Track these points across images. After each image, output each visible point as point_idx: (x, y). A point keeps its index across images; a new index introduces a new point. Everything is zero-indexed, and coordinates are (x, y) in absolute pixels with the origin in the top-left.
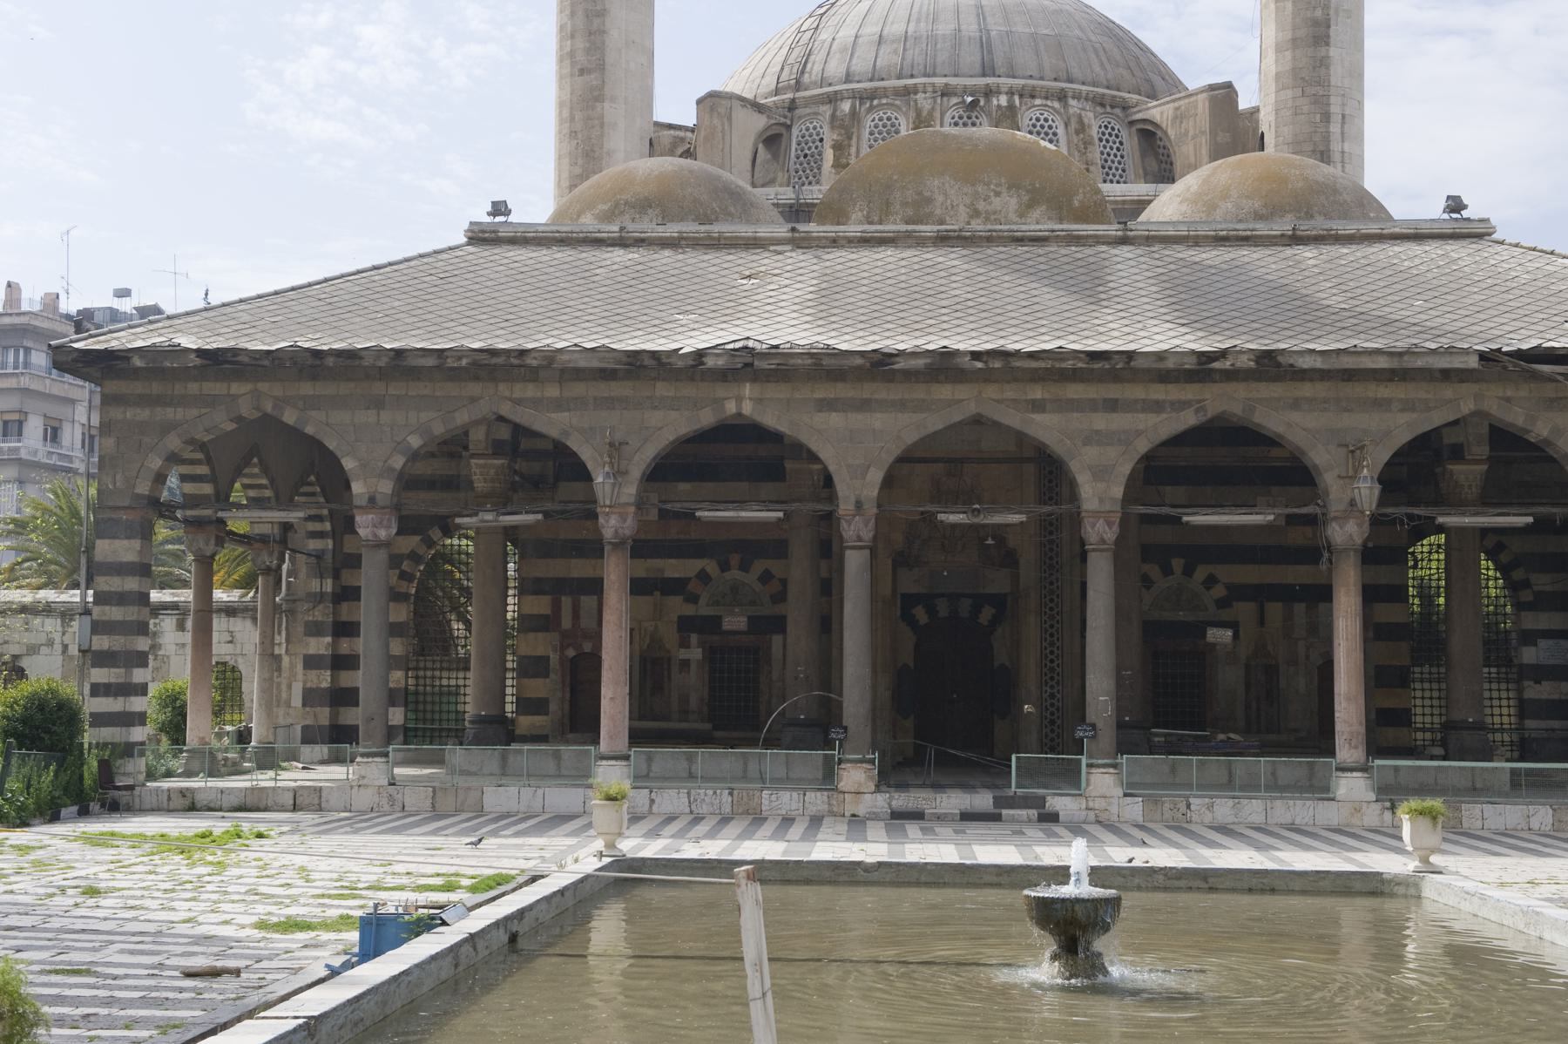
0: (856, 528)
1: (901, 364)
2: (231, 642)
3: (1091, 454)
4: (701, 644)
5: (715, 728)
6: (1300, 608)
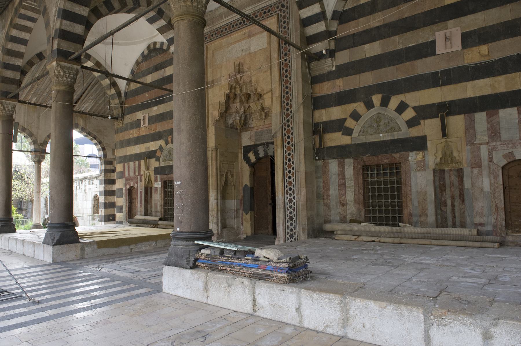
2: (96, 188)
4: (161, 180)
5: (161, 219)
6: (481, 117)
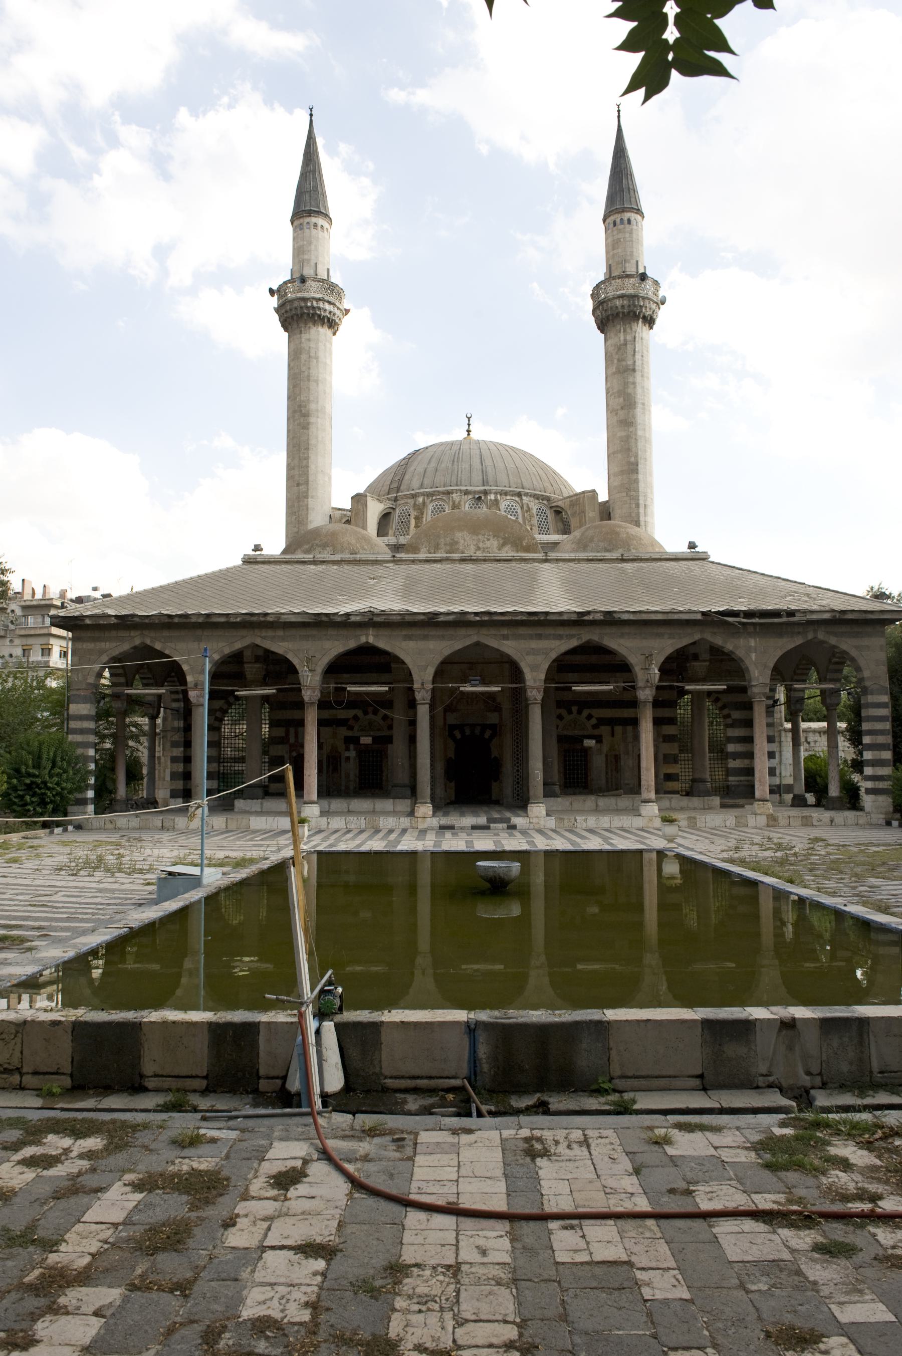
0: (423, 696)
1: (442, 618)
3: (530, 659)
